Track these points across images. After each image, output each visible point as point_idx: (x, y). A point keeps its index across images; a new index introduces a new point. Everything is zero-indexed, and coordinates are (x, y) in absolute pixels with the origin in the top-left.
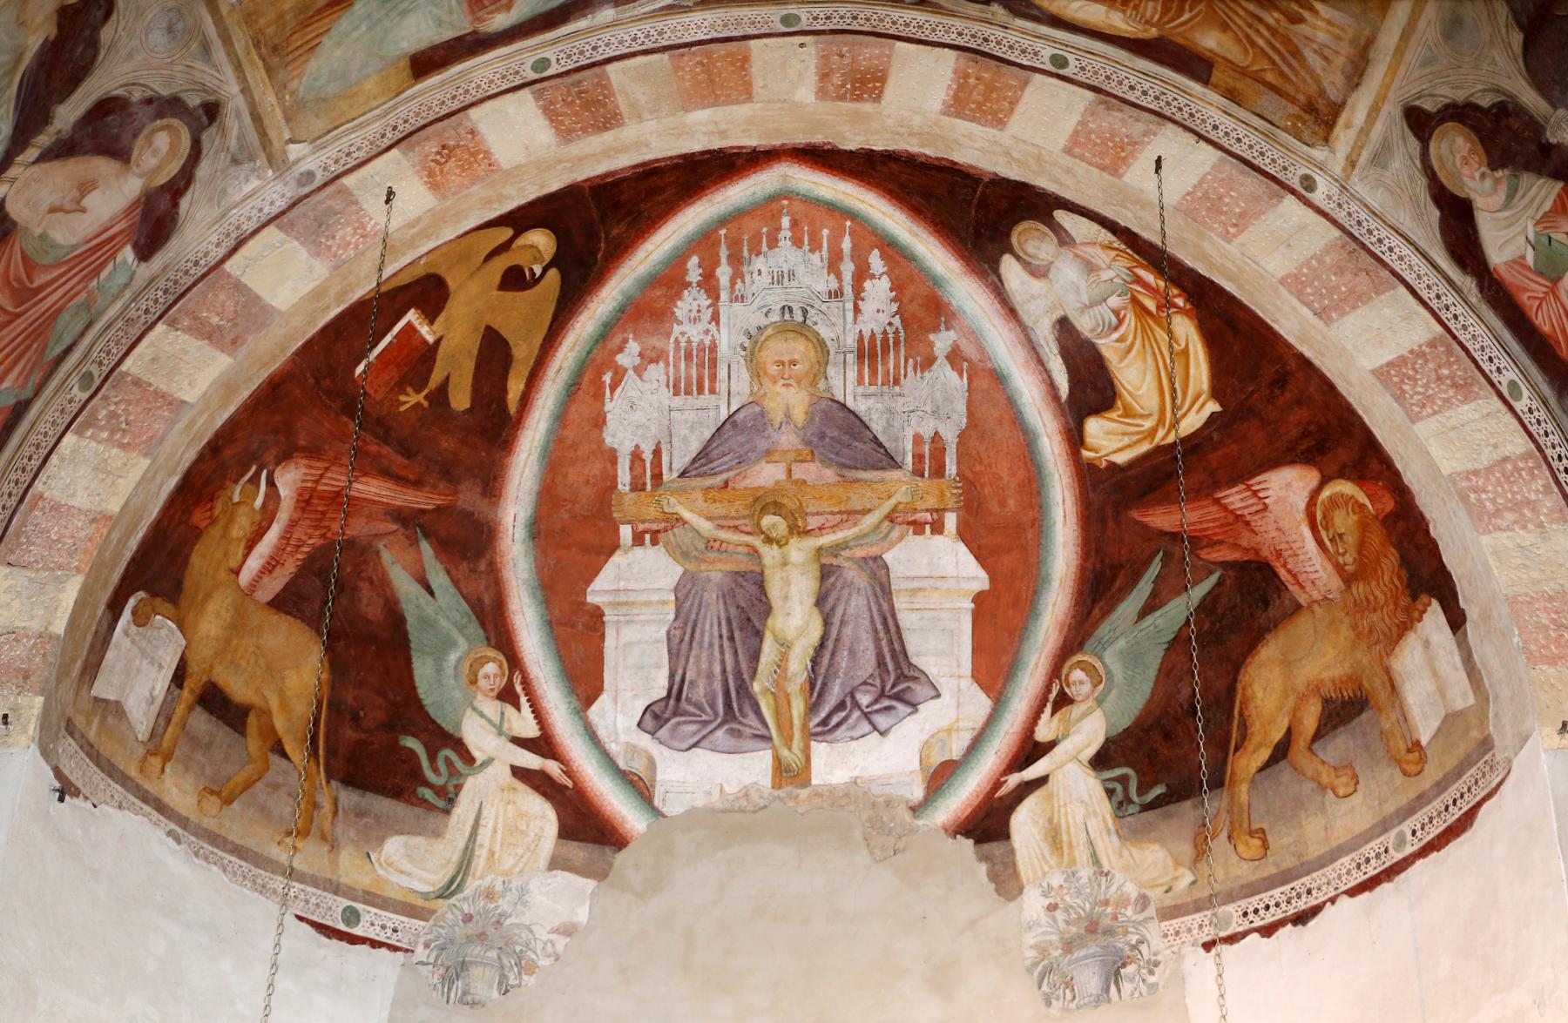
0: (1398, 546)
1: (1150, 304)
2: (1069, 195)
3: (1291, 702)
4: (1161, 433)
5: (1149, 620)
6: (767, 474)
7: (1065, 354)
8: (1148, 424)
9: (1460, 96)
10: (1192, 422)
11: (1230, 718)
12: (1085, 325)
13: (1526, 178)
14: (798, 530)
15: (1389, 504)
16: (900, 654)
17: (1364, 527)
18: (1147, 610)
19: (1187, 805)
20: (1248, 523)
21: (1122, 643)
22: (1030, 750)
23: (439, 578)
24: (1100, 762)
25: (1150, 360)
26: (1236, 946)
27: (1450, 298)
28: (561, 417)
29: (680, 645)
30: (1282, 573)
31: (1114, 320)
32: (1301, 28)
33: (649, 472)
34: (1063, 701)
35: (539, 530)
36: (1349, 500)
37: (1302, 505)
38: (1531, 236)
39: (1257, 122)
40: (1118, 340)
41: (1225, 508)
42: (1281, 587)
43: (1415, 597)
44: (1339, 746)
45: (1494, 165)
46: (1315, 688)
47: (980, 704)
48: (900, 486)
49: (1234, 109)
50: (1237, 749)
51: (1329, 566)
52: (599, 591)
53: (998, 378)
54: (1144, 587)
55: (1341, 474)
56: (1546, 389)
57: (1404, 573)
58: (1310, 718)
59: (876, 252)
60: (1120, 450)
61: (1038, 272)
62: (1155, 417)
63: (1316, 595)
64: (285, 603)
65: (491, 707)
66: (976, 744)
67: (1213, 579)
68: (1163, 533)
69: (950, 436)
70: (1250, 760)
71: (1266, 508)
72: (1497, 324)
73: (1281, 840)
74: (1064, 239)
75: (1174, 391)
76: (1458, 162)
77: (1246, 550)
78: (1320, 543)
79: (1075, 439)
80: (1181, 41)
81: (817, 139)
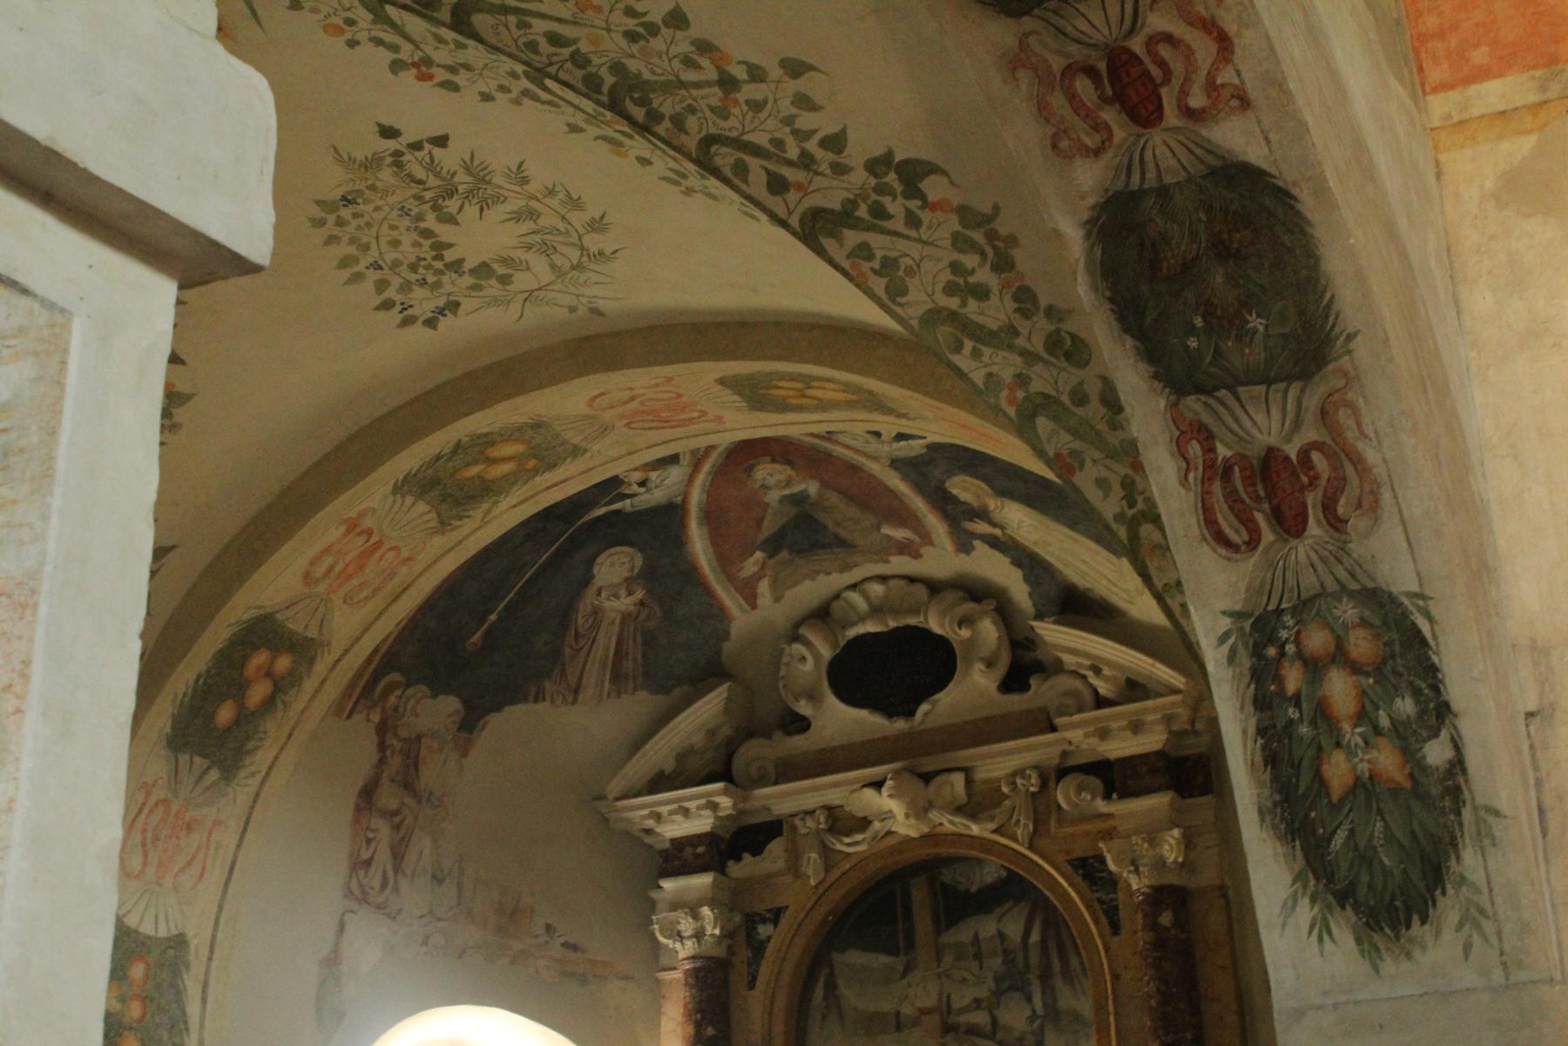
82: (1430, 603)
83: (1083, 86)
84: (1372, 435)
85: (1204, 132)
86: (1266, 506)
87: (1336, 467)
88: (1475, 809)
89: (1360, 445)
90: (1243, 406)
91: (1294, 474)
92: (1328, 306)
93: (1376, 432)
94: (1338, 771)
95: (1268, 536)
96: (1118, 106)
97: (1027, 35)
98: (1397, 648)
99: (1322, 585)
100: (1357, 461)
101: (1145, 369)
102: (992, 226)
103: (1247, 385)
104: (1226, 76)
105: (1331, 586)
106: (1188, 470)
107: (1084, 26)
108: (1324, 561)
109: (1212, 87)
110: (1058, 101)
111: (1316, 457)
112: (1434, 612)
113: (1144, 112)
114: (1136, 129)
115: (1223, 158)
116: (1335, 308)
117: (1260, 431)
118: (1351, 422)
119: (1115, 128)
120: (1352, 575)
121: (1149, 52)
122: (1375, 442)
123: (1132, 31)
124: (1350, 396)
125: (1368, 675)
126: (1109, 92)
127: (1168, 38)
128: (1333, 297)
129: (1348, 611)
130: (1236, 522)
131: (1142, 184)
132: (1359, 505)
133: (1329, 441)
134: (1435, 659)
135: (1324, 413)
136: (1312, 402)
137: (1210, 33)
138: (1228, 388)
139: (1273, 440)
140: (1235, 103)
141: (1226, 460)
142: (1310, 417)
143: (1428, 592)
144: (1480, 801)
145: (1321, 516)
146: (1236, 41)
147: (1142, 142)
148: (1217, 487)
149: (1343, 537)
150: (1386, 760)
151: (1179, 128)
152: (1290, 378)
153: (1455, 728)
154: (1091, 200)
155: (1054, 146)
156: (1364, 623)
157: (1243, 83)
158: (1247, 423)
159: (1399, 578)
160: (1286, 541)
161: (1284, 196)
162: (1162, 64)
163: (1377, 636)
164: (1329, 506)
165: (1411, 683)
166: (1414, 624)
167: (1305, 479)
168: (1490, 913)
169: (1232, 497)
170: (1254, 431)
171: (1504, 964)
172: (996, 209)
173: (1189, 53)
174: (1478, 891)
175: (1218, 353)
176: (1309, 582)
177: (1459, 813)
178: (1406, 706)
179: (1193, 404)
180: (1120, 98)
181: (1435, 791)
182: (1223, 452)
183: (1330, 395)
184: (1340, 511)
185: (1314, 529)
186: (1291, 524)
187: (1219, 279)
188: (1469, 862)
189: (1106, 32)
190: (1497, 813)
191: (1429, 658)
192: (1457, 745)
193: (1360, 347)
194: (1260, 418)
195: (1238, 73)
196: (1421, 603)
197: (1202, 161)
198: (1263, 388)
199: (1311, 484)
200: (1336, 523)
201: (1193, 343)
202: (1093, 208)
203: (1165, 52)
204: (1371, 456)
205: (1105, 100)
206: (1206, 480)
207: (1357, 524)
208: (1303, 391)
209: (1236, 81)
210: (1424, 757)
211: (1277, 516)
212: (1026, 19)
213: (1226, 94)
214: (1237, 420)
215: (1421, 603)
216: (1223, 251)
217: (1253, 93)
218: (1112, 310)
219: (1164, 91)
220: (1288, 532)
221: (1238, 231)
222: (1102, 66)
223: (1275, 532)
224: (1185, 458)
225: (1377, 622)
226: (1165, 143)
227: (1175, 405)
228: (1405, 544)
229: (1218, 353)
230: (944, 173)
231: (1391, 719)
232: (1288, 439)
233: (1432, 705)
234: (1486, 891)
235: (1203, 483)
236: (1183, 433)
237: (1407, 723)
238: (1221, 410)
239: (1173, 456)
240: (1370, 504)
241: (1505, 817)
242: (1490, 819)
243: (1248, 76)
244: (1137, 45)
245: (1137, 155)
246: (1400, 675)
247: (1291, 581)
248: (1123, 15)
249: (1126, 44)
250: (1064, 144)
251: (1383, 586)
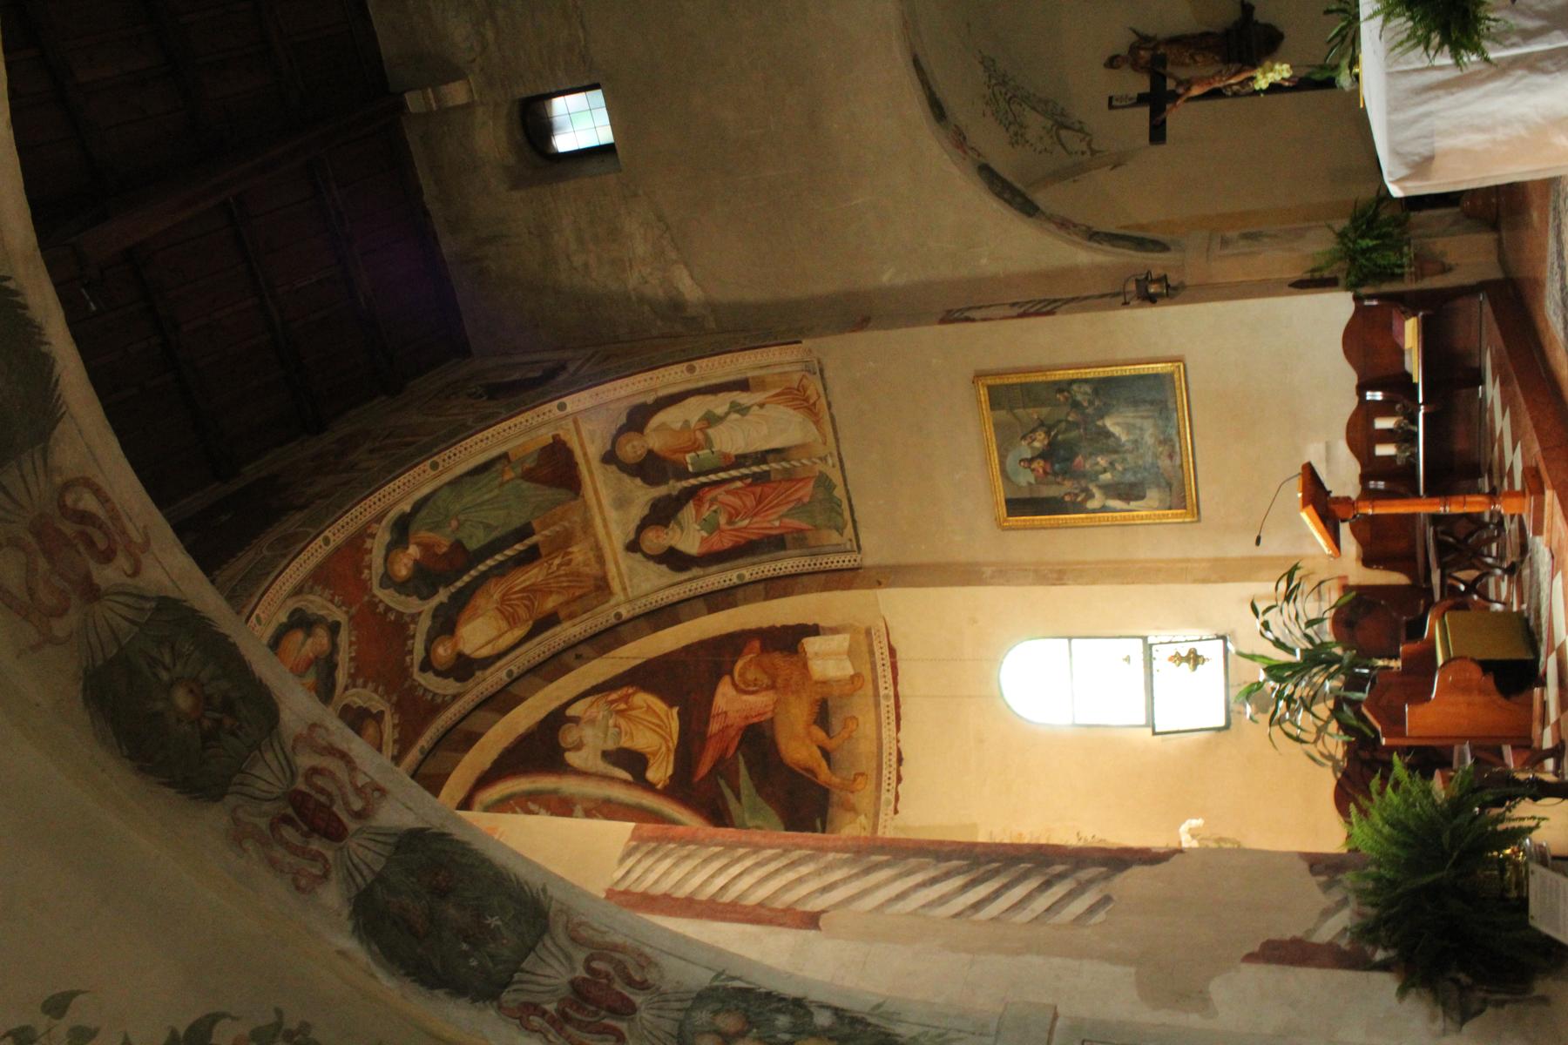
0: (775, 650)
1: (623, 706)
2: (564, 700)
3: (808, 742)
4: (671, 745)
5: (744, 799)
7: (616, 764)
8: (664, 749)
9: (637, 522)
10: (675, 725)
11: (802, 776)
12: (610, 745)
13: (680, 515)
15: (757, 644)
17: (760, 665)
18: (738, 797)
19: (831, 811)
20: (727, 727)
21: (747, 816)
25: (641, 727)
26: (901, 798)
27: (694, 585)
30: (755, 720)
31: (617, 729)
32: (573, 564)
36: (744, 668)
37: (734, 693)
38: (698, 528)
39: (585, 616)
40: (626, 734)
41: (715, 735)
42: (759, 724)
43: (796, 652)
44: (836, 722)
45: (666, 526)
46: (809, 725)
49: (578, 620)
50: (816, 776)
51: (764, 693)
54: (728, 792)
55: (734, 663)
56: (750, 560)
57: (786, 653)
58: (819, 734)
59: (529, 803)
60: (667, 768)
61: (578, 747)
62: (664, 742)
63: (771, 708)
67: (741, 758)
68: (710, 772)
70: (824, 774)
71: (726, 713)
72: (714, 568)
73: (863, 769)
74: (575, 720)
75: (658, 726)
76: (655, 541)
77: (737, 734)
78: (753, 693)
79: (649, 787)
80: (541, 616)
81: (477, 773)
82: (727, 972)
83: (288, 832)
84: (607, 929)
85: (374, 824)
86: (603, 1013)
87: (611, 960)
88: (869, 1014)
89: (608, 939)
90: (534, 974)
91: (596, 984)
92: (518, 880)
93: (606, 926)
95: (623, 1026)
96: (316, 836)
97: (234, 810)
98: (744, 1005)
99: (677, 1020)
100: (615, 948)
101: (464, 1002)
102: (284, 1027)
103: (523, 960)
104: (361, 780)
105: (681, 1015)
106: (545, 1036)
107: (265, 787)
108: (660, 1009)
109: (359, 791)
110: (279, 853)
111: (595, 965)
112: (733, 974)
113: (335, 832)
114: (337, 845)
115: (395, 834)
116: (522, 881)
117: (556, 978)
118: (591, 932)
119: (324, 852)
120: (681, 1000)
121: (310, 786)
122: (612, 932)
123: (293, 775)
124: (576, 920)
125: (749, 1031)
126: (305, 828)
127: (315, 771)
128: (515, 875)
129: (702, 1017)
130: (600, 1037)
131: (365, 880)
132: (643, 967)
133: (593, 951)
134: (762, 990)
135: (573, 940)
136: (563, 940)
137: (334, 755)
138: (516, 972)
139: (568, 977)
140: (376, 794)
141: (557, 1010)
142: (571, 950)
143: (721, 970)
144: (867, 1009)
145: (632, 990)
146: (351, 754)
147: (346, 853)
148: (569, 1029)
149: (654, 988)
151: (359, 829)
152: (540, 937)
153: (811, 1002)
154: (346, 912)
155: (298, 888)
156: (716, 1013)
157: (372, 779)
158: (546, 981)
159: (701, 978)
160: (632, 1020)
161: (442, 837)
162: (322, 791)
163: (728, 1011)
164: (630, 982)
165: (771, 1011)
166: (734, 988)
167: (604, 981)
168: (944, 1031)
169: (581, 1026)
170: (553, 981)
171: (981, 1034)
172: (279, 1012)
173: (332, 775)
174: (926, 1033)
175: (492, 957)
176: (669, 1026)
177: (869, 1024)
178: (783, 1021)
179: (507, 997)
180: (314, 830)
181: (847, 1030)
182: (551, 1007)
183: (567, 928)
184: (637, 978)
185: (638, 999)
186: (626, 1009)
187: (452, 912)
189: (278, 784)
190: (879, 1006)
191: (760, 994)
192: (823, 1006)
193: (551, 890)
194: (548, 971)
195: (365, 774)
196: (723, 977)
197: (385, 843)
198: (532, 956)
199: (609, 980)
200: (643, 986)
201: (474, 963)
202: (350, 918)
203: (319, 781)
204: (618, 939)
205: (306, 835)
206: (560, 1031)
207: (652, 976)
208: (552, 938)
209: (368, 780)
210: (822, 1026)
211: (614, 1012)
212: (228, 798)
213: (368, 790)
214: (539, 984)
215: (723, 977)
216: (442, 893)
217: (382, 783)
218: (414, 981)
219: (335, 809)
220: (628, 1014)
221: (437, 874)
222: (290, 811)
223: (623, 1020)
224: (536, 1031)
225: (719, 1005)
226: (360, 845)
227: (500, 1007)
228: (683, 963)
229: (492, 957)
230: (223, 1015)
231: (785, 1032)
232: (573, 969)
233: (791, 1007)
234: (927, 1029)
235: (560, 1034)
236: (520, 1018)
237: (795, 1025)
238: (525, 986)
239: (529, 1036)
240: (646, 962)
241: (884, 1002)
242: (881, 1009)
243: (371, 773)
244: (300, 784)
245: (349, 863)
246: (760, 1013)
247: (661, 1035)
248: (282, 767)
249: (294, 787)
250: (303, 882)
251: (699, 989)
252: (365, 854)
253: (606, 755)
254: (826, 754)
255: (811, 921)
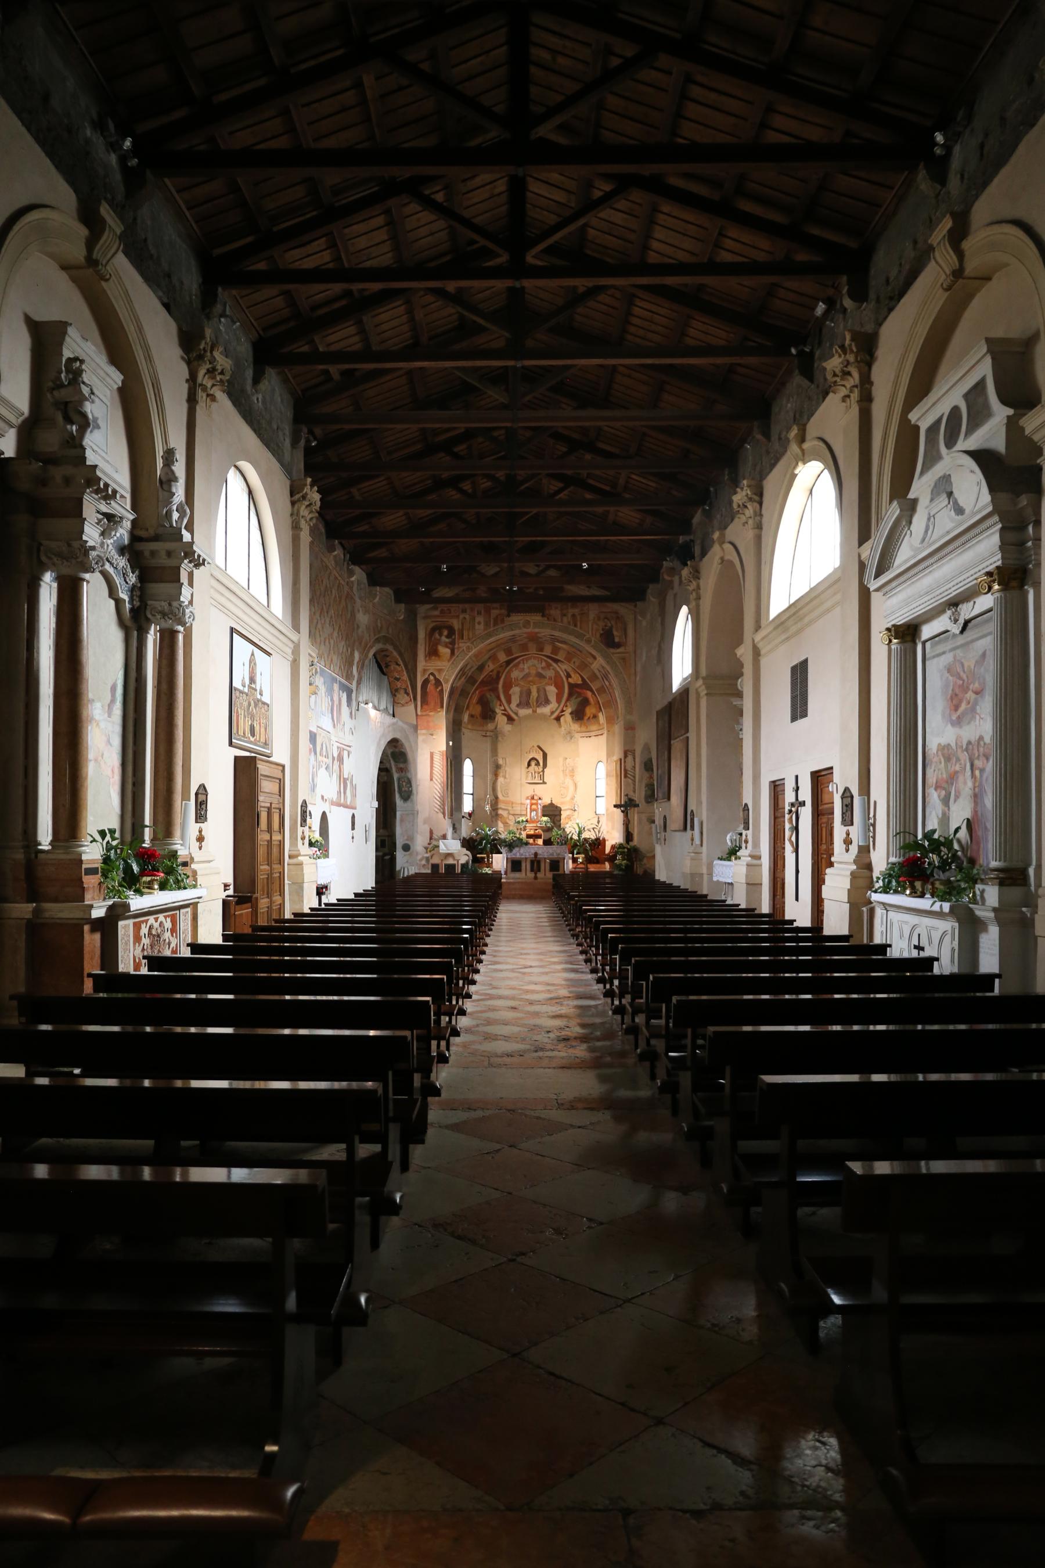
6: (531, 679)
14: (535, 684)
16: (547, 698)
22: (563, 711)
23: (492, 694)
24: (571, 713)
28: (506, 676)
29: (520, 697)
33: (517, 679)
34: (566, 706)
35: (503, 686)
47: (557, 705)
48: (546, 681)
52: (511, 692)
53: (559, 672)
58: (592, 716)
64: (477, 703)
65: (498, 707)
66: (557, 710)
69: (553, 675)
70: (586, 718)
79: (567, 679)
94: (403, 789)
150: (407, 789)
159: (410, 777)
186: (402, 772)
188: (412, 797)
252: (397, 750)
253: (565, 670)
254: (589, 718)
255: (431, 780)
